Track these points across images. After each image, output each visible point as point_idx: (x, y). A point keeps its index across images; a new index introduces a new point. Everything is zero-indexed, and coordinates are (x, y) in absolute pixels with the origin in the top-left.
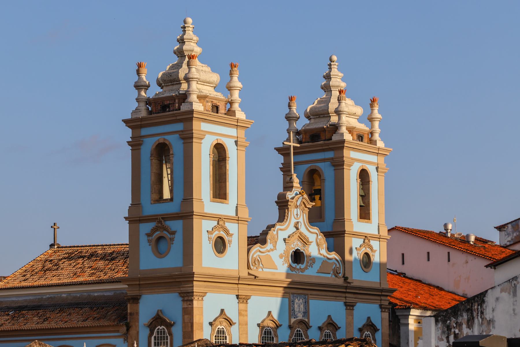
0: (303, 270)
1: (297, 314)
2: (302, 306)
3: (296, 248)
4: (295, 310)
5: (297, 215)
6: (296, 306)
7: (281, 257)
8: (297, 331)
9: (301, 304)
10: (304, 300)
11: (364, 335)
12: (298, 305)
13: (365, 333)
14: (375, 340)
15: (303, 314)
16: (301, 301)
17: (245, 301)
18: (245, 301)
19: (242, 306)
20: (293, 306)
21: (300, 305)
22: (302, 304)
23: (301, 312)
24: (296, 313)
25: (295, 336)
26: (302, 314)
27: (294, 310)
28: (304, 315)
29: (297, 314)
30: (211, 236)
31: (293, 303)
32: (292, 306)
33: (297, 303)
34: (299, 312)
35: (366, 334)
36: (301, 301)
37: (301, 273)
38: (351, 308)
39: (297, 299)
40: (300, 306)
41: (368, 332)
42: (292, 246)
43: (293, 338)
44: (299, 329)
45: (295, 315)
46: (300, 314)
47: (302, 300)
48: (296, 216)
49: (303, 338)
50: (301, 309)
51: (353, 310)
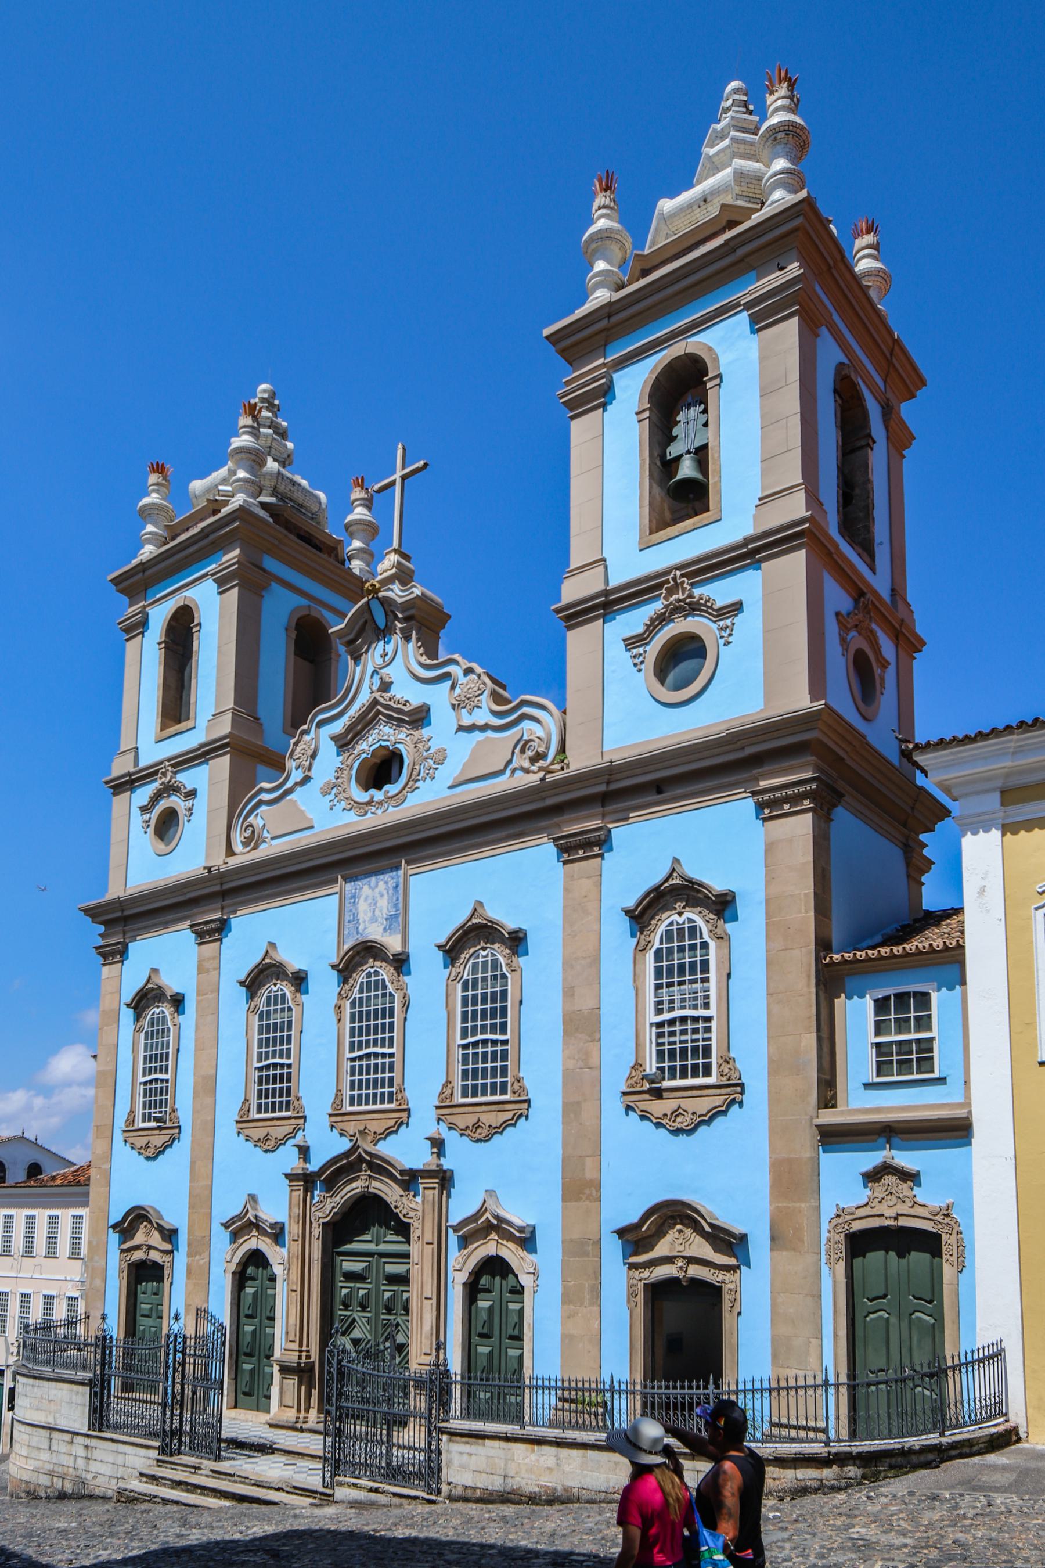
1: (365, 929)
4: (358, 920)
9: (382, 895)
10: (390, 883)
12: (370, 901)
15: (385, 922)
20: (354, 911)
21: (378, 898)
22: (386, 896)
23: (379, 920)
24: (361, 928)
25: (361, 991)
26: (382, 924)
27: (355, 919)
28: (390, 925)
29: (365, 929)
30: (146, 817)
31: (354, 902)
32: (351, 911)
33: (366, 899)
34: (374, 920)
39: (366, 887)
40: (375, 904)
43: (355, 998)
44: (372, 970)
45: (358, 933)
46: (376, 924)
47: (386, 883)
49: (390, 993)
50: (381, 911)
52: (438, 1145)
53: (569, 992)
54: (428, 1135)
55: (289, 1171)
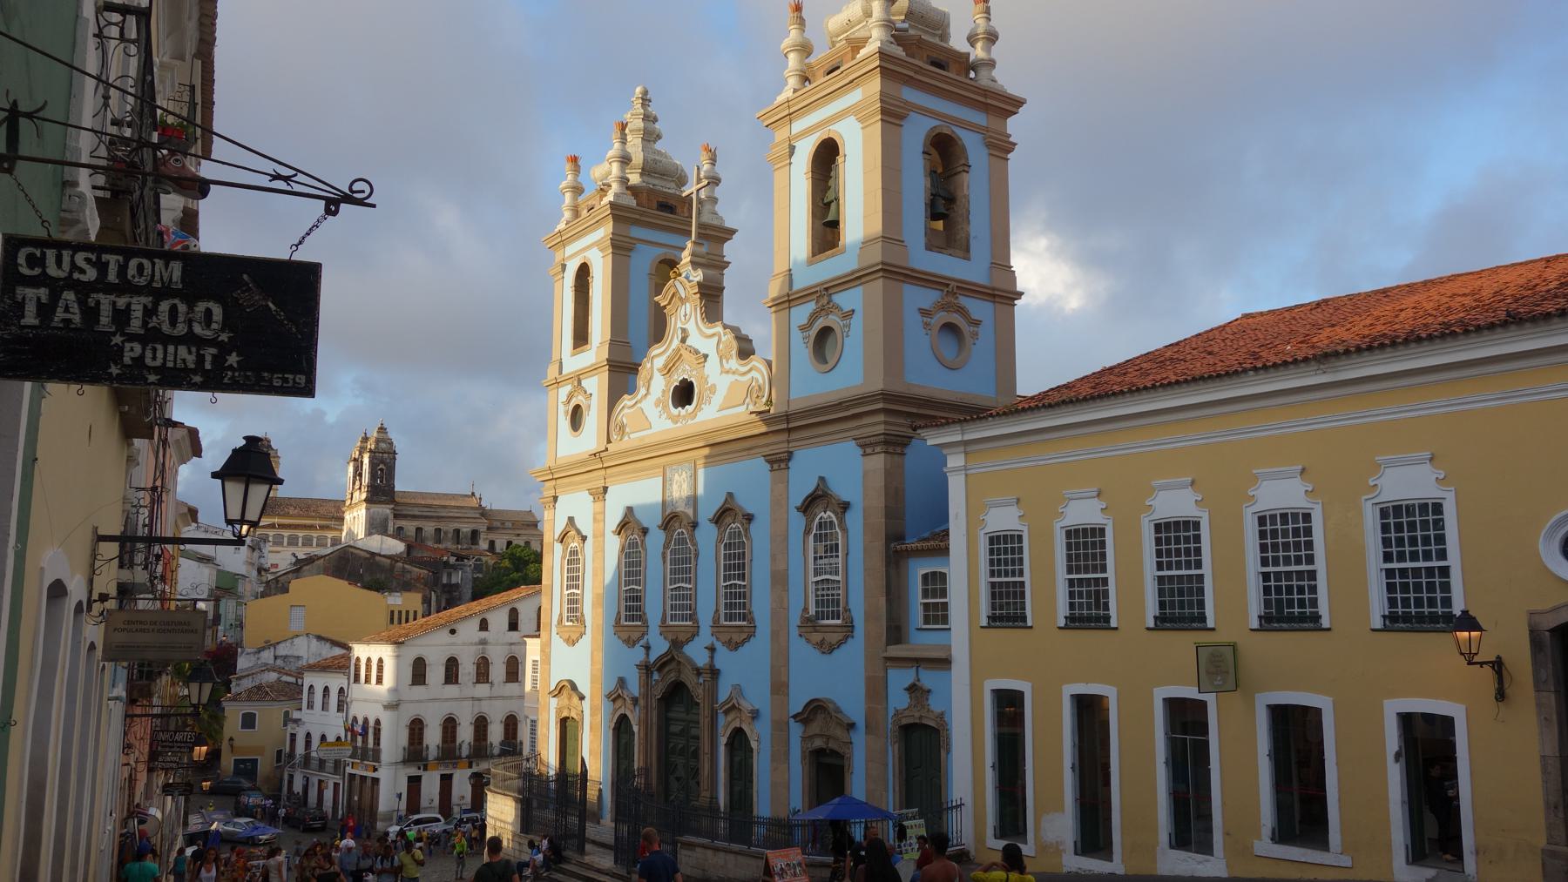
0: (693, 415)
2: (685, 486)
3: (681, 378)
5: (686, 315)
6: (675, 487)
7: (657, 403)
8: (679, 534)
11: (817, 520)
13: (819, 517)
14: (845, 530)
16: (684, 475)
17: (601, 497)
18: (601, 497)
19: (599, 504)
35: (821, 518)
36: (684, 475)
37: (690, 422)
38: (783, 466)
39: (676, 474)
41: (828, 513)
42: (676, 377)
44: (680, 530)
48: (683, 318)
51: (903, 454)
52: (712, 649)
53: (773, 558)
54: (706, 645)
55: (638, 663)
